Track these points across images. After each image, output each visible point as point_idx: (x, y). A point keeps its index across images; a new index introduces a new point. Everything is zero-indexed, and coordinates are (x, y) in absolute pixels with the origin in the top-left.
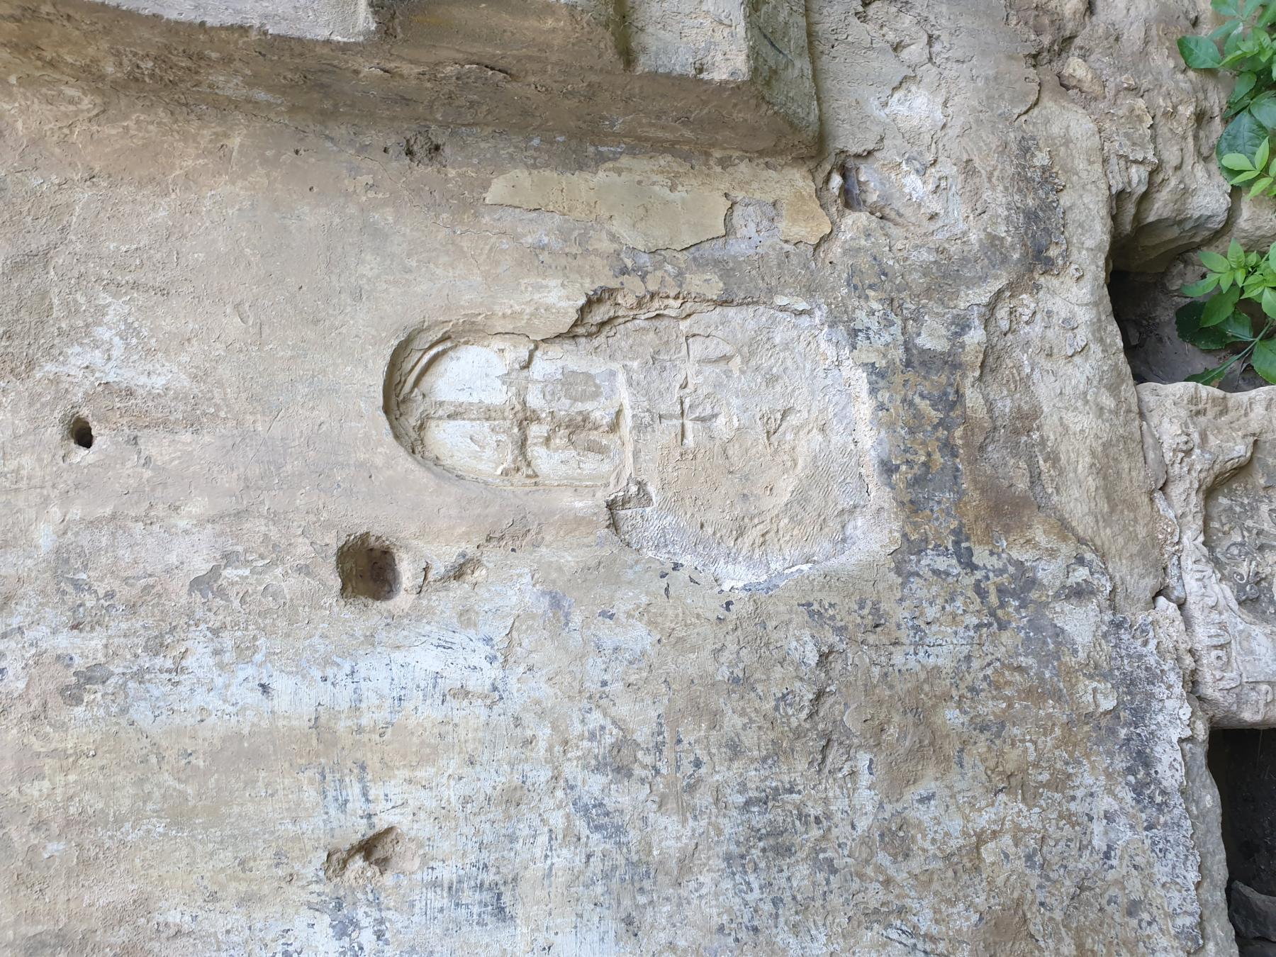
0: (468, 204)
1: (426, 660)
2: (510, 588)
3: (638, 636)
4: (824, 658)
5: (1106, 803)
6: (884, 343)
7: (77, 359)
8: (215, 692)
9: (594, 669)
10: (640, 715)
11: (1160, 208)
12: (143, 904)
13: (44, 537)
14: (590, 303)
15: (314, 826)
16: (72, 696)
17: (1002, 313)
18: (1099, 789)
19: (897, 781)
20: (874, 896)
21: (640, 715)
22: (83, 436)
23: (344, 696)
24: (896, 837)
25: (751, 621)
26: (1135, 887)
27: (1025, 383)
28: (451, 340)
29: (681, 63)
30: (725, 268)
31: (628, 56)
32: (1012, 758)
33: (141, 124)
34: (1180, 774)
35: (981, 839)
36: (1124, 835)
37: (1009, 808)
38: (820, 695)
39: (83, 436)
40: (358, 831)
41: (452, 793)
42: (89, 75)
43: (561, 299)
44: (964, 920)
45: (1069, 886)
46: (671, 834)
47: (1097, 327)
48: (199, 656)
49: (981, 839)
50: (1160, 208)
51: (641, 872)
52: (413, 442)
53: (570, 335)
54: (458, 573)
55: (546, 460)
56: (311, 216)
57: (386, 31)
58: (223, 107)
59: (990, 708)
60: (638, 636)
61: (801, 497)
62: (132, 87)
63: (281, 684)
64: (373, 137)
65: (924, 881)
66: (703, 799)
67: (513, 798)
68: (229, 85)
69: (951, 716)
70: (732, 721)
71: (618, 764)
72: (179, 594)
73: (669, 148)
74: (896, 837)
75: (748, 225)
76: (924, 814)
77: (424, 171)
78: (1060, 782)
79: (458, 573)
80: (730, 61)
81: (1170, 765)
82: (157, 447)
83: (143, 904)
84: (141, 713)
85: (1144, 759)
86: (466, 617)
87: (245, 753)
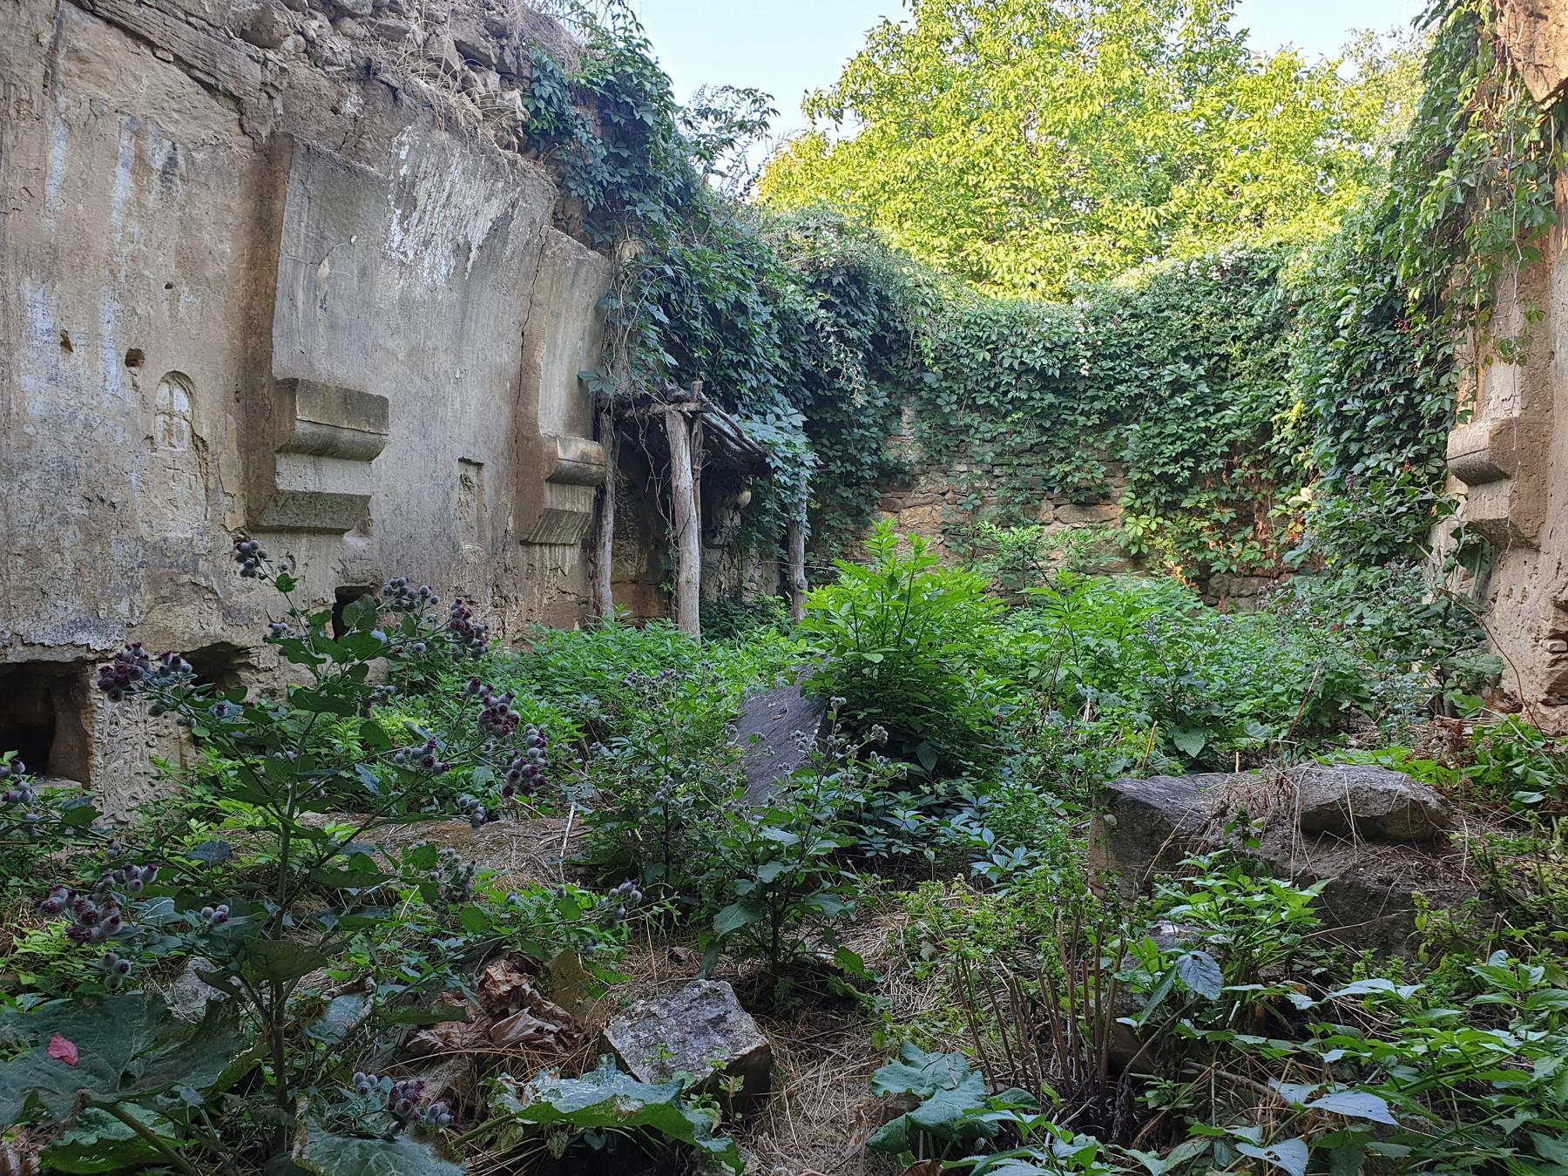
0: (226, 408)
1: (113, 371)
2: (131, 400)
3: (119, 440)
4: (113, 505)
5: (70, 609)
6: (201, 545)
7: (187, 289)
8: (109, 308)
9: (111, 423)
10: (98, 435)
11: (245, 675)
12: (61, 279)
13: (146, 273)
14: (203, 442)
15: (74, 329)
16: (111, 271)
17: (210, 596)
18: (72, 607)
19: (81, 523)
20: (48, 509)
21: (98, 435)
22: (168, 286)
23: (106, 344)
24: (64, 521)
25: (120, 481)
26: (44, 616)
27: (190, 602)
28: (190, 395)
29: (279, 468)
30: (215, 490)
31: (278, 452)
32: (85, 571)
33: (239, 317)
34: (78, 643)
35: (62, 554)
36: (61, 614)
37: (70, 568)
38: (103, 500)
39: (168, 286)
40: (72, 342)
41: (81, 371)
42: (250, 307)
43: (204, 433)
44: (39, 542)
45: (46, 588)
46: (69, 439)
47: (207, 636)
48: (117, 306)
49: (62, 554)
50: (245, 675)
51: (58, 427)
52: (164, 380)
53: (194, 434)
54: (134, 385)
55: (160, 418)
56: (220, 359)
57: (278, 383)
58: (244, 340)
59: (99, 565)
60: (119, 440)
61: (155, 507)
62: (248, 318)
63: (110, 327)
64: (240, 382)
65: (51, 528)
66: (78, 452)
67: (78, 389)
68: (252, 342)
69: (98, 549)
70: (97, 467)
71: (88, 426)
72: (133, 304)
73: (247, 477)
74: (64, 521)
75: (227, 501)
76: (70, 532)
77: (233, 396)
78: (77, 590)
79: (134, 385)
80: (282, 484)
81: (81, 638)
82: (166, 305)
83: (61, 279)
84: (105, 288)
85: (84, 628)
86: (123, 385)
87: (94, 313)
